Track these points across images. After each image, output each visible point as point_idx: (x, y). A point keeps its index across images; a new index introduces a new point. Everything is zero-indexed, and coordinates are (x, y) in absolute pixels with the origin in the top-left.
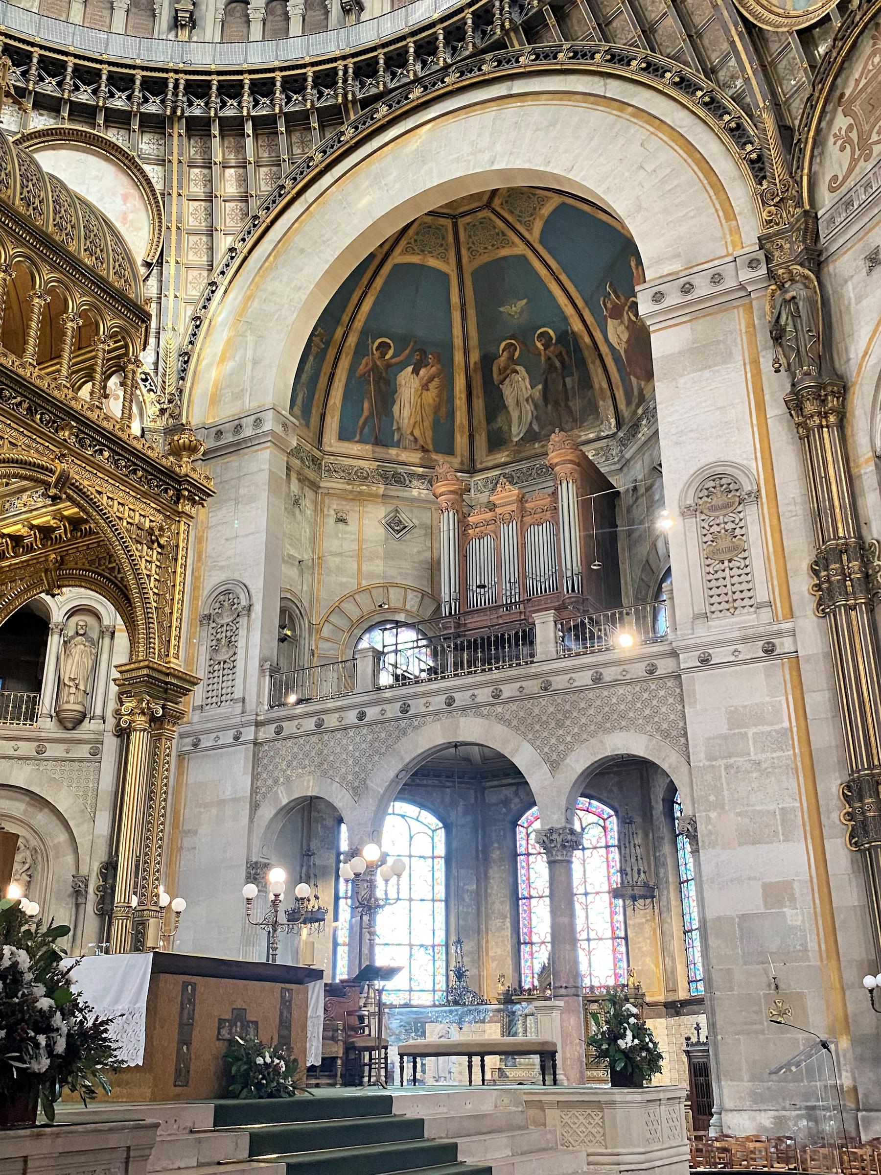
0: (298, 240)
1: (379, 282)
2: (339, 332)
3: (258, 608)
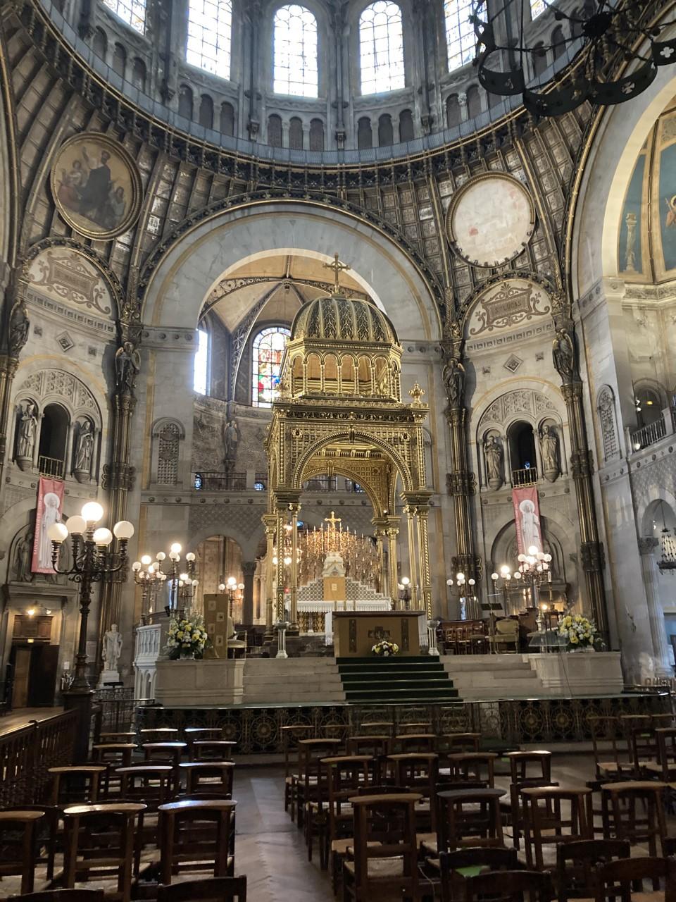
0: (599, 172)
1: (657, 166)
2: (644, 208)
3: (617, 398)
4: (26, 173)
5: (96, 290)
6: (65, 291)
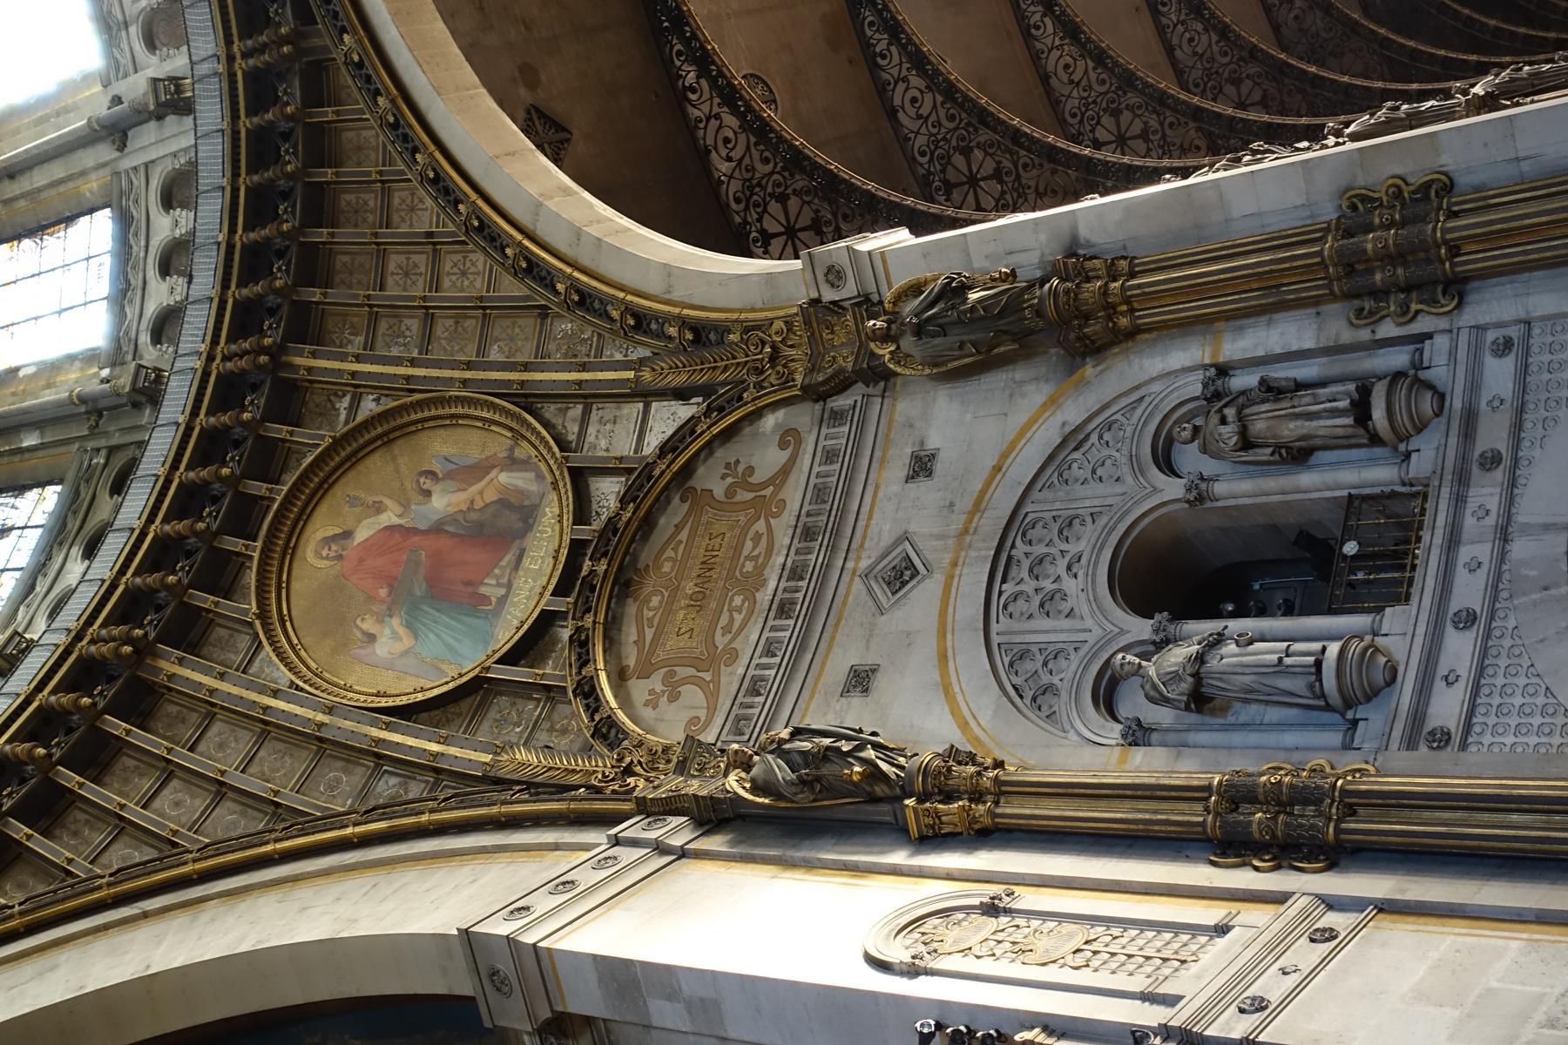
4: (387, 787)
5: (730, 492)
6: (738, 600)
